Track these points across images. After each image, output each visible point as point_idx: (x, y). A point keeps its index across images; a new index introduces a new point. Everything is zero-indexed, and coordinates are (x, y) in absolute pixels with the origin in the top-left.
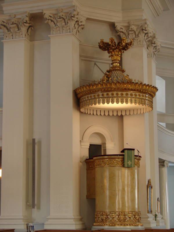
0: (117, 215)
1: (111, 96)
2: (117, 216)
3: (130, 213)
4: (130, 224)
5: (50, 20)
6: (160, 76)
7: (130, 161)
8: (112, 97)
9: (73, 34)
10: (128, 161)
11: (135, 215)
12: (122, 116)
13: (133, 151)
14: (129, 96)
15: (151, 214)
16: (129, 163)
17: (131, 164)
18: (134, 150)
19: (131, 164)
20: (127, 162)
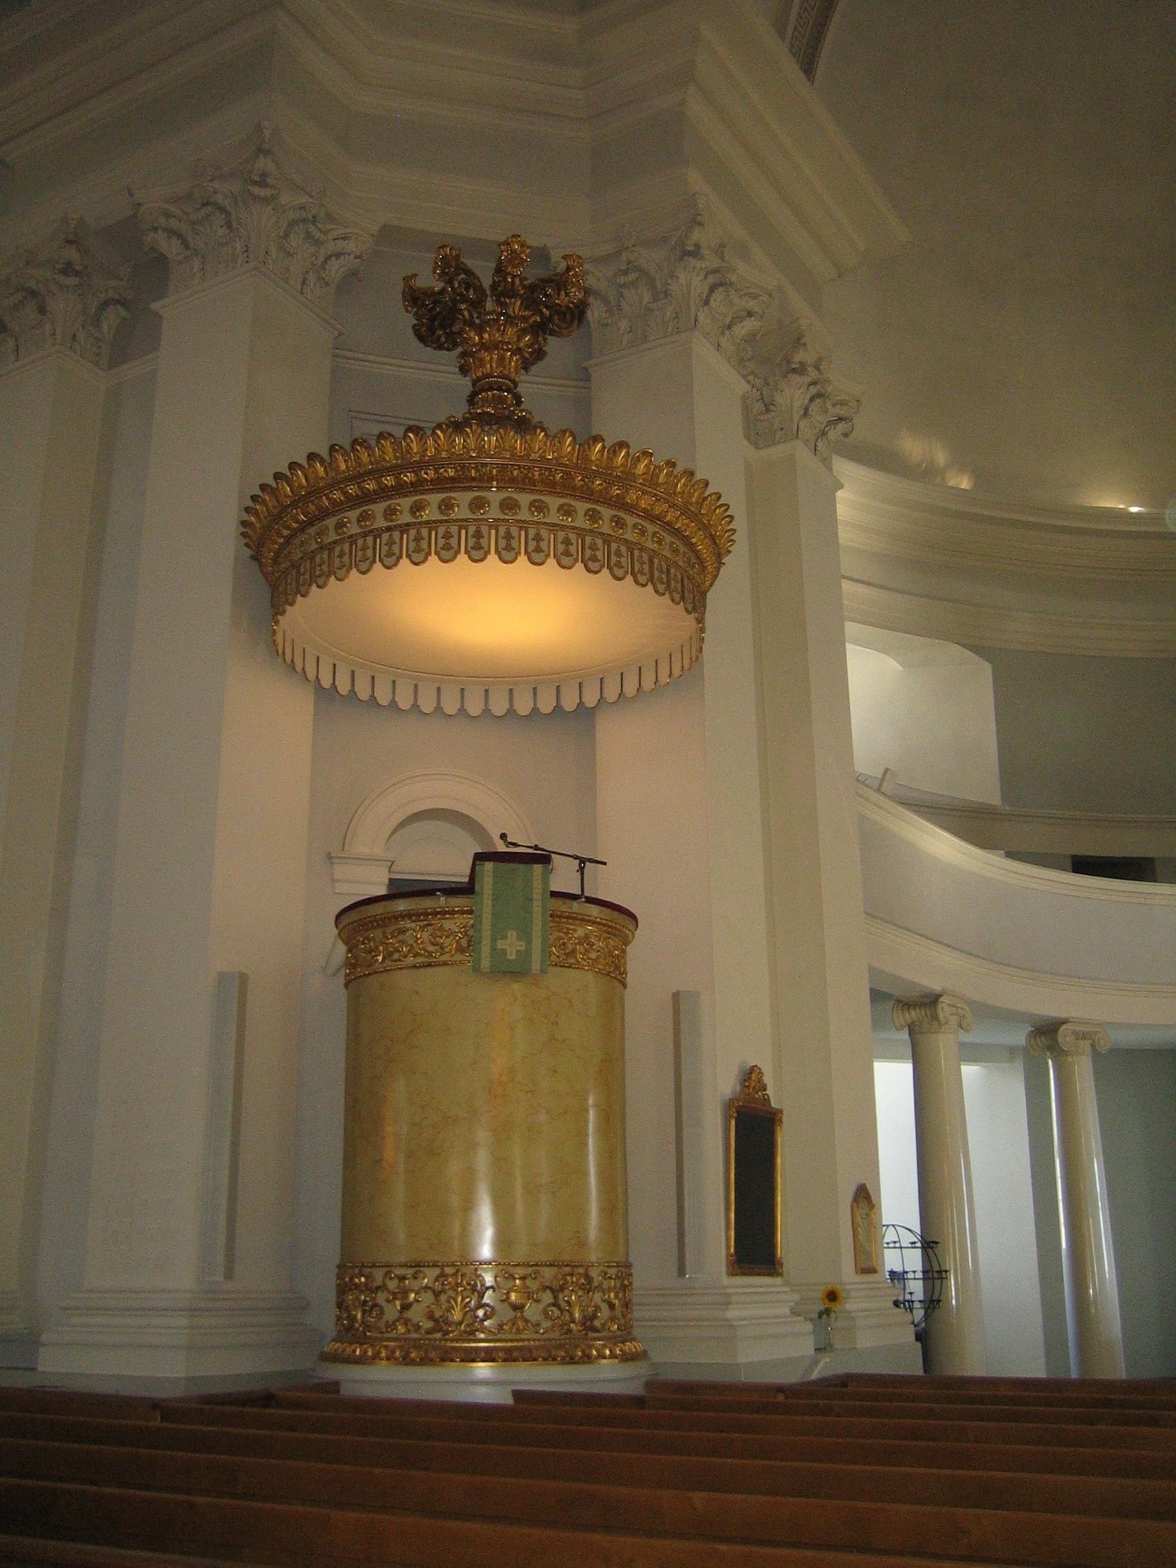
0: (426, 1288)
1: (381, 523)
2: (428, 1298)
3: (519, 1272)
4: (508, 1351)
5: (160, 232)
6: (964, 646)
7: (512, 935)
8: (389, 529)
9: (256, 269)
10: (498, 934)
11: (562, 1289)
12: (585, 715)
13: (537, 869)
14: (494, 513)
15: (779, 1280)
16: (512, 945)
17: (525, 956)
18: (543, 858)
19: (525, 956)
20: (494, 940)
